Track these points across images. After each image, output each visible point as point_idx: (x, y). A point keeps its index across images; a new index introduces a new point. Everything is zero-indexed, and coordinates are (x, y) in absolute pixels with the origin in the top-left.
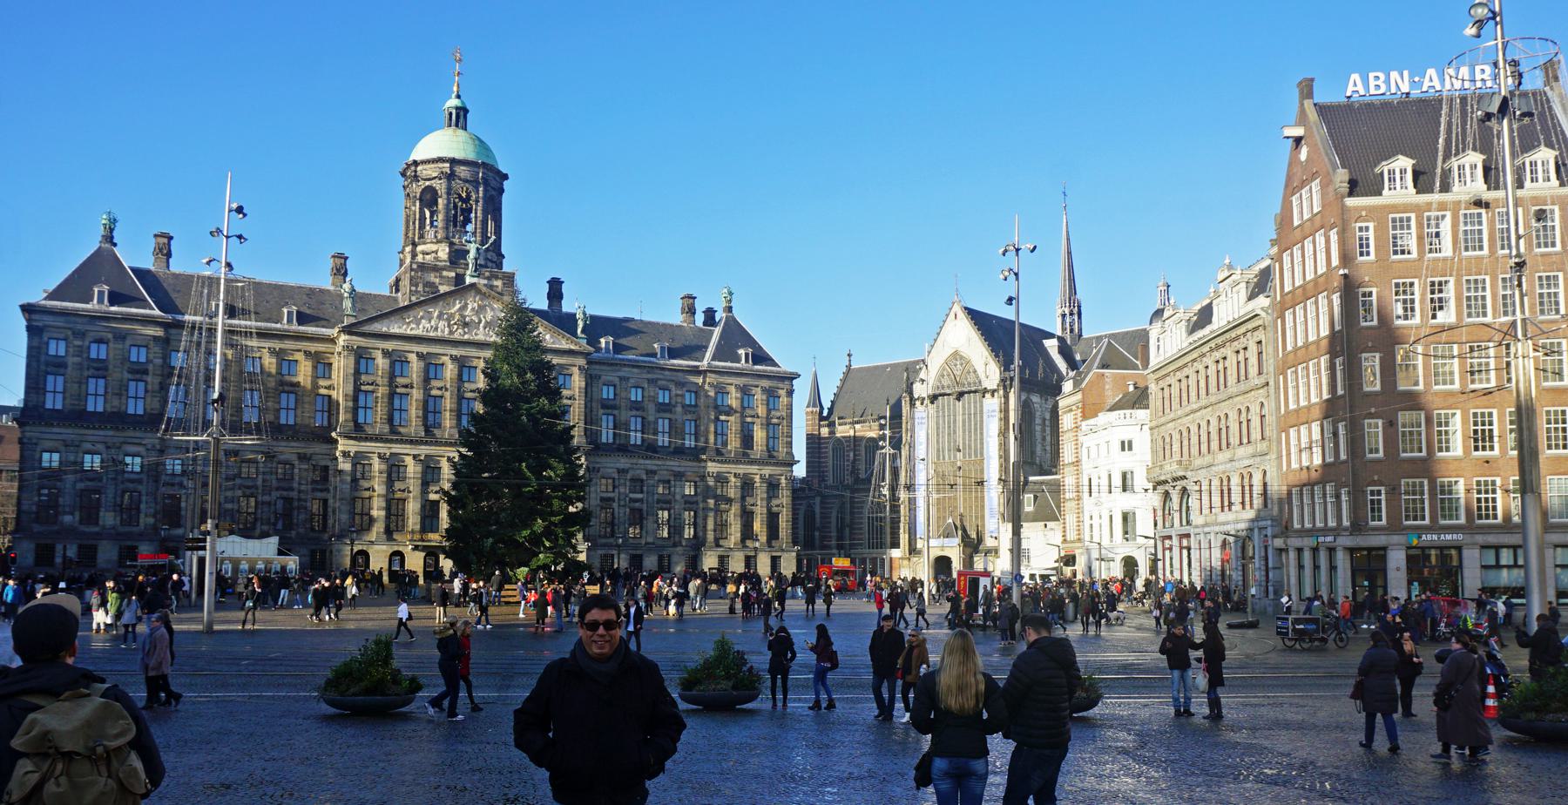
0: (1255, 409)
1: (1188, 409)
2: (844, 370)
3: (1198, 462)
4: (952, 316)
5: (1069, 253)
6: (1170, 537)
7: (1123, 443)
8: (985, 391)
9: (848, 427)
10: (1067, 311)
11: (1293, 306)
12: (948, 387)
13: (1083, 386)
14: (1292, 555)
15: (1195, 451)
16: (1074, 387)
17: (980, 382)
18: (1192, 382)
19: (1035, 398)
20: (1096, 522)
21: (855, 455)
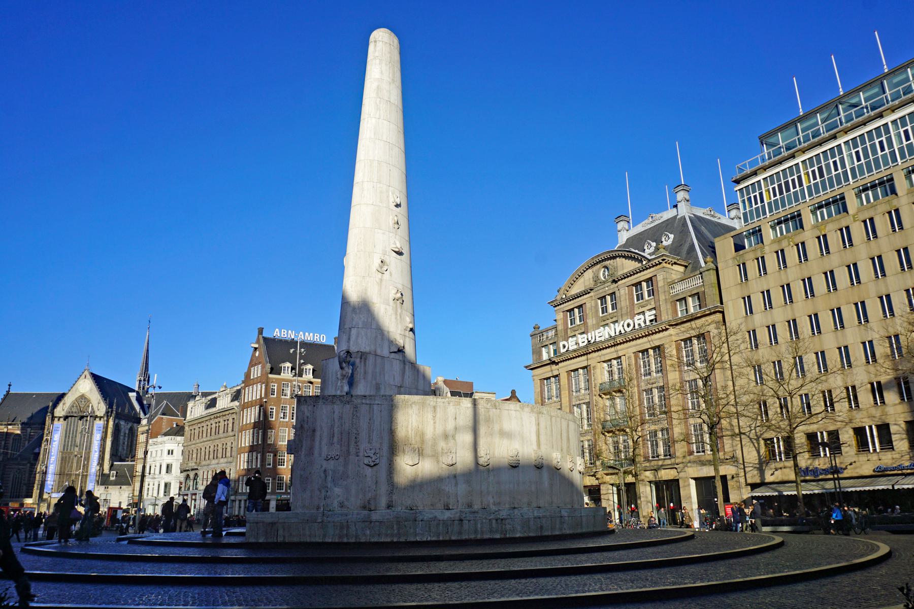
0: (229, 444)
1: (202, 440)
2: (5, 393)
3: (204, 463)
4: (83, 376)
5: (148, 350)
6: (187, 495)
7: (169, 451)
8: (96, 417)
9: (3, 427)
10: (142, 379)
11: (247, 408)
12: (75, 412)
13: (152, 422)
14: (237, 503)
15: (203, 458)
16: (148, 422)
17: (94, 412)
18: (205, 429)
19: (122, 423)
20: (151, 487)
21: (5, 443)
